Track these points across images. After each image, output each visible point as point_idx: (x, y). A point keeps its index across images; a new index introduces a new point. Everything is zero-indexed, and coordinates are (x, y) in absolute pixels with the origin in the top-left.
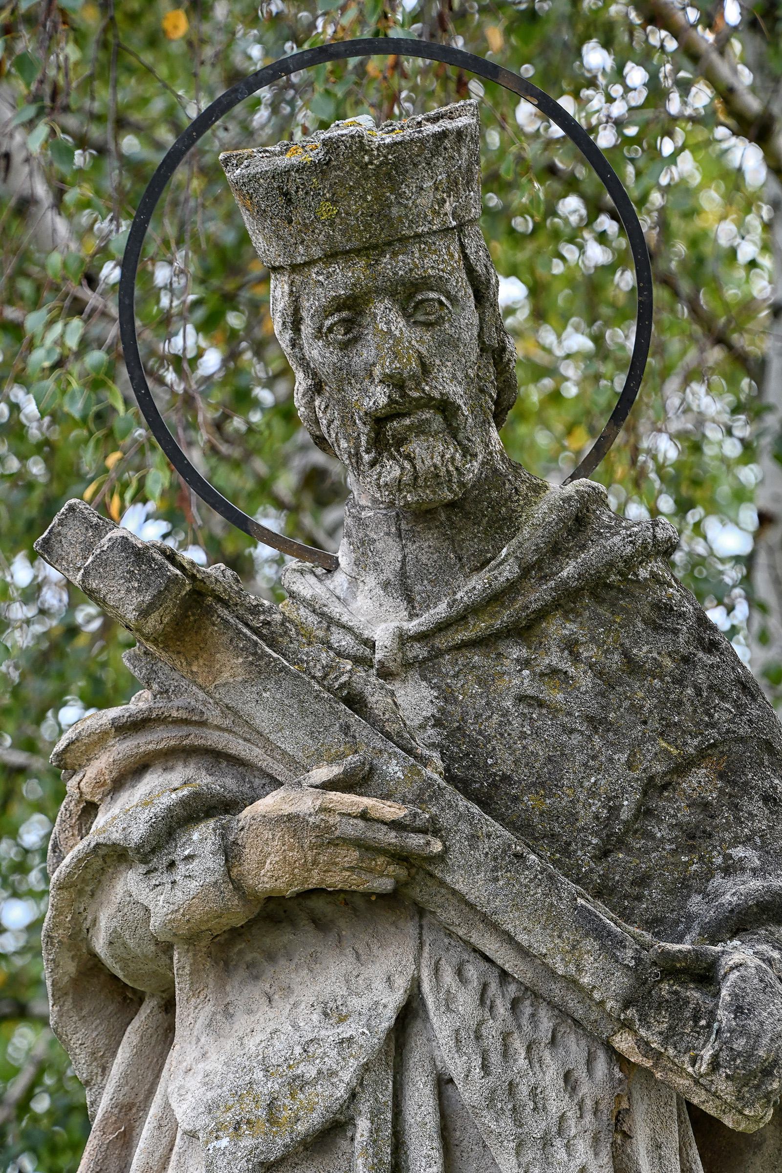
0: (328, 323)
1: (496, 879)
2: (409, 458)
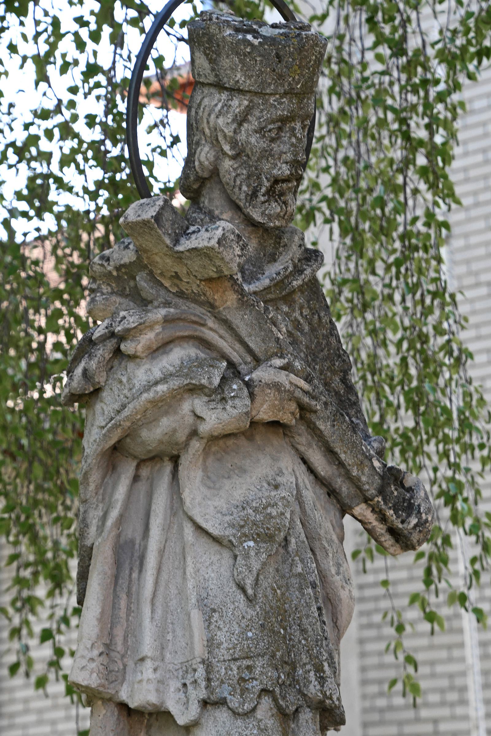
0: (272, 126)
1: (334, 426)
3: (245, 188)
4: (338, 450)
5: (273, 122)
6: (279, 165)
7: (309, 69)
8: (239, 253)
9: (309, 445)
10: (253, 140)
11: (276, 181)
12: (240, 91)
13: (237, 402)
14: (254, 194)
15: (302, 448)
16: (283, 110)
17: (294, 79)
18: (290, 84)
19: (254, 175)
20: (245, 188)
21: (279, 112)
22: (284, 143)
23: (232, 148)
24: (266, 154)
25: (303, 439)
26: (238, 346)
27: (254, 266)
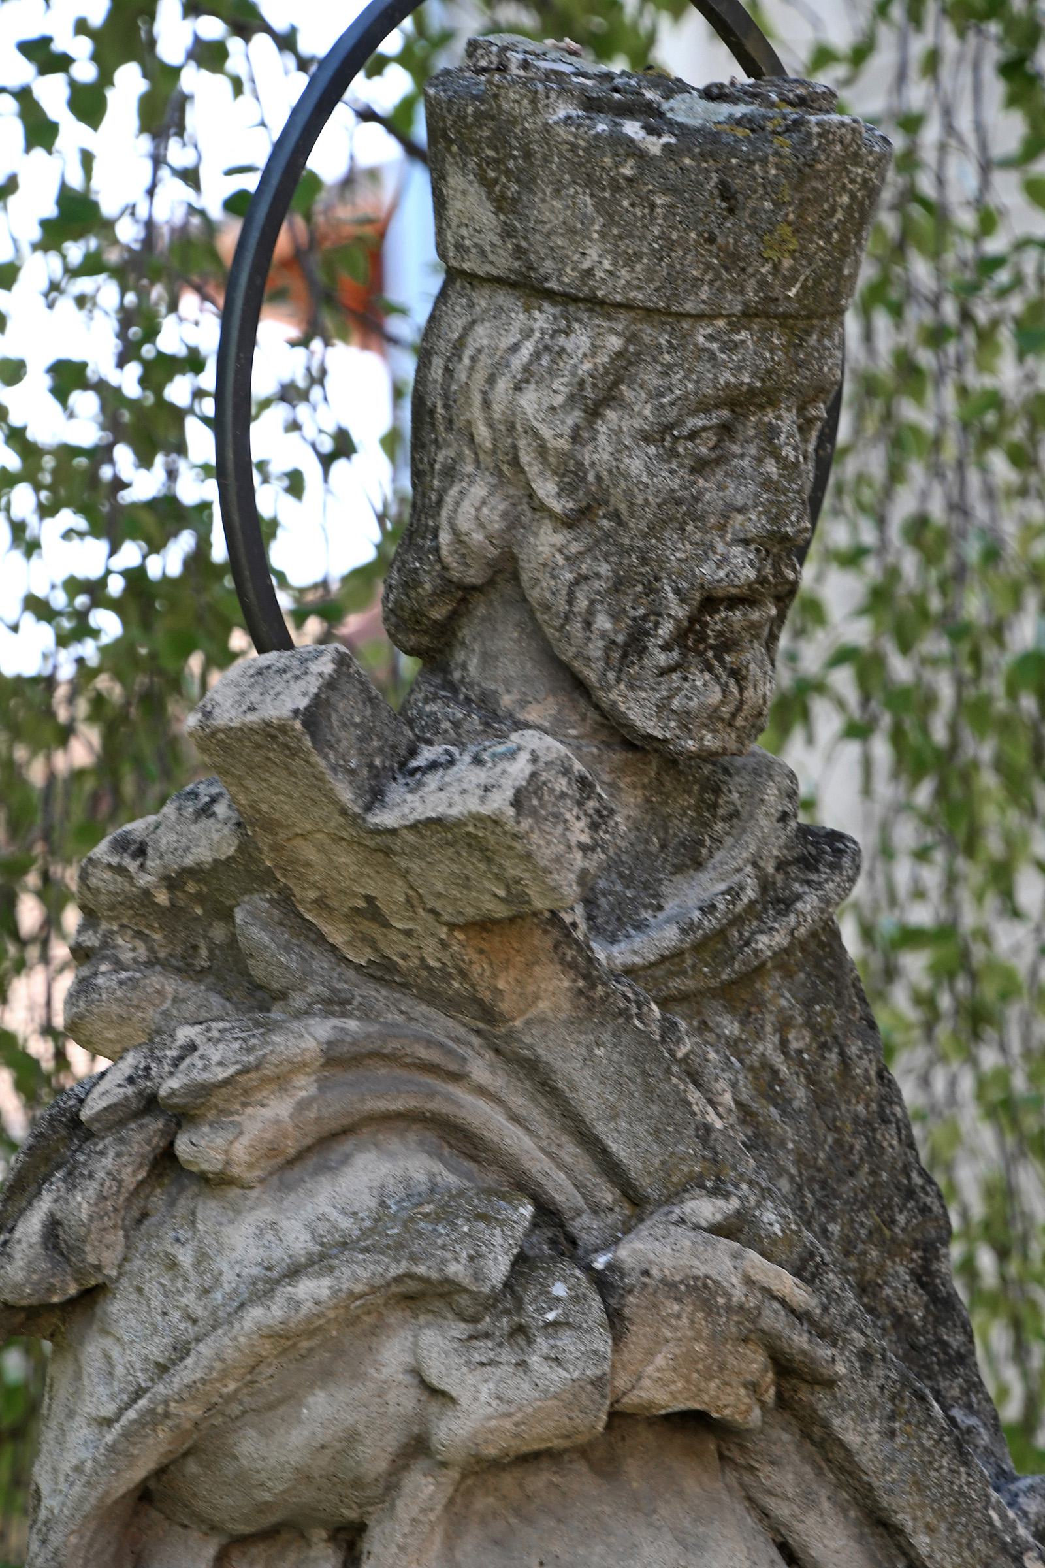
0: (699, 422)
1: (892, 1434)
2: (737, 674)
3: (603, 622)
4: (903, 1519)
5: (704, 407)
6: (720, 547)
7: (827, 236)
8: (585, 838)
9: (809, 1501)
10: (635, 465)
11: (710, 603)
12: (595, 304)
13: (566, 1340)
14: (635, 643)
15: (782, 1510)
16: (740, 368)
17: (776, 268)
18: (763, 284)
19: (637, 581)
20: (603, 622)
21: (726, 377)
22: (740, 476)
23: (566, 490)
24: (680, 512)
25: (786, 1477)
26: (570, 1151)
27: (627, 880)
